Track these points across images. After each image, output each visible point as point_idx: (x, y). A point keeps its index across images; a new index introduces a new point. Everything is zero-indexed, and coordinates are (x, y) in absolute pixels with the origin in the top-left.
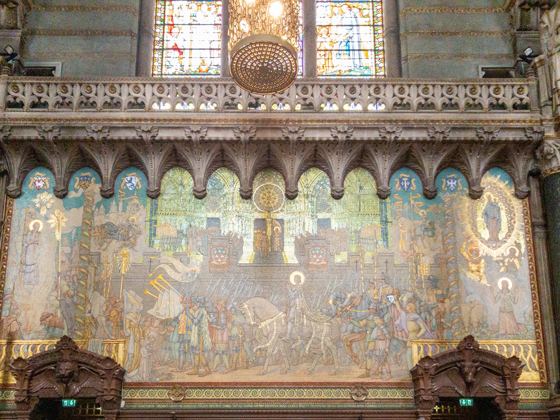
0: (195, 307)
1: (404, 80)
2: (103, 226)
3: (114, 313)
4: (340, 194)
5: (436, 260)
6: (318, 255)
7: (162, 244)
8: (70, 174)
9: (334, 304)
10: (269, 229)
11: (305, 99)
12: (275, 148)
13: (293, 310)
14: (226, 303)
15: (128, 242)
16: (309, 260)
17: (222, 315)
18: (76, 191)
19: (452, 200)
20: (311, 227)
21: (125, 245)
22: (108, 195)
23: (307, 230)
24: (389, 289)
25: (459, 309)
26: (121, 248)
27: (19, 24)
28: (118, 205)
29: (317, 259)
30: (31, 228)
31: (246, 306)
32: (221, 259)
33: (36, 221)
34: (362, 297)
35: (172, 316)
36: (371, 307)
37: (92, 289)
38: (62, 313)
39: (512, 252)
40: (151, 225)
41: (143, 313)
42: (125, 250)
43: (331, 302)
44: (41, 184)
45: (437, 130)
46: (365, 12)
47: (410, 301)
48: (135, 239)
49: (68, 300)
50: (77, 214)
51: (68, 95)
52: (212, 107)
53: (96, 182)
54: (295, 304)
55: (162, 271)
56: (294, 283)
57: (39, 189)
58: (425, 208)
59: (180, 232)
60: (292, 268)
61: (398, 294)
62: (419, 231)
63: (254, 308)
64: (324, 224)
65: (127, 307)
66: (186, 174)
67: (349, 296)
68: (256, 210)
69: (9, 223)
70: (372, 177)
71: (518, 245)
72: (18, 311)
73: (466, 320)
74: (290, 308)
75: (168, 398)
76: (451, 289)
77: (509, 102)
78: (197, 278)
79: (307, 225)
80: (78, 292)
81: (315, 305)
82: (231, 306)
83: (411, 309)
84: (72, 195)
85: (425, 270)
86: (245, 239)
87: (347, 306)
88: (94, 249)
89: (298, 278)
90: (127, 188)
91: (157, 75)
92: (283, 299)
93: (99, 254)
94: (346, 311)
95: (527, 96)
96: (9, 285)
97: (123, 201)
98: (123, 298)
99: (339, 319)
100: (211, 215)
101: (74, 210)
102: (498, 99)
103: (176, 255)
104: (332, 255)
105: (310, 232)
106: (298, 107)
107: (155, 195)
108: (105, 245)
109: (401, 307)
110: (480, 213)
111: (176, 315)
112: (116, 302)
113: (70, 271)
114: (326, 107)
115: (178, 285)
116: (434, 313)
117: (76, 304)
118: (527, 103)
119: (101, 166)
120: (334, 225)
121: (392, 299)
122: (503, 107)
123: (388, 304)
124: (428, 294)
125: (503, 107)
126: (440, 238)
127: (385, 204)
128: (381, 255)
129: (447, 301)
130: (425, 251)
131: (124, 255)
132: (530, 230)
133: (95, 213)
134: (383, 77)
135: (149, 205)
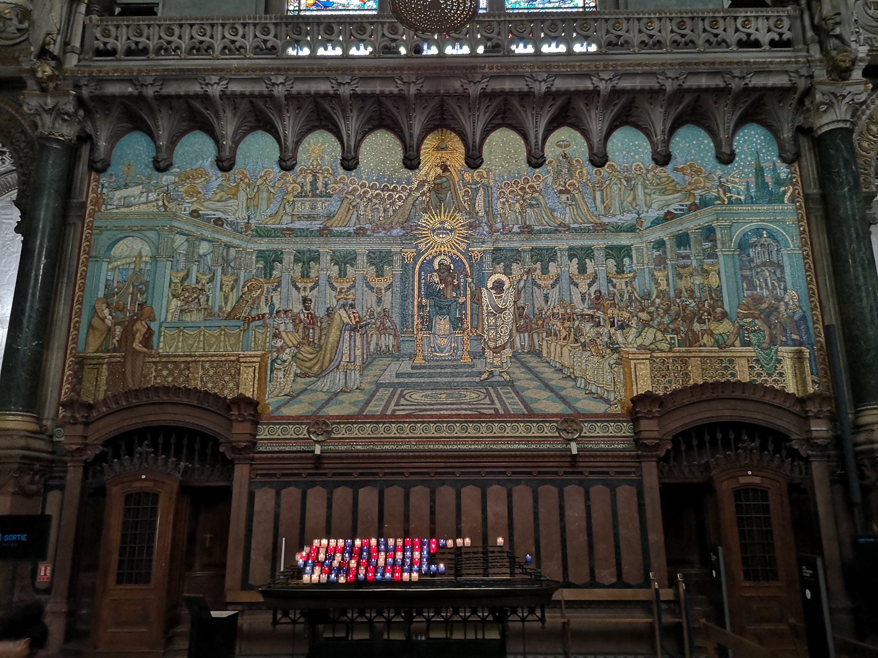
1: (620, 13)
4: (540, 161)
11: (489, 39)
12: (452, 104)
45: (669, 75)
51: (175, 38)
52: (363, 51)
75: (307, 436)
77: (765, 38)
91: (294, 11)
95: (789, 30)
102: (749, 35)
106: (481, 50)
114: (520, 49)
118: (789, 40)
122: (756, 44)
125: (756, 44)
132: (803, 204)
134: (594, 9)
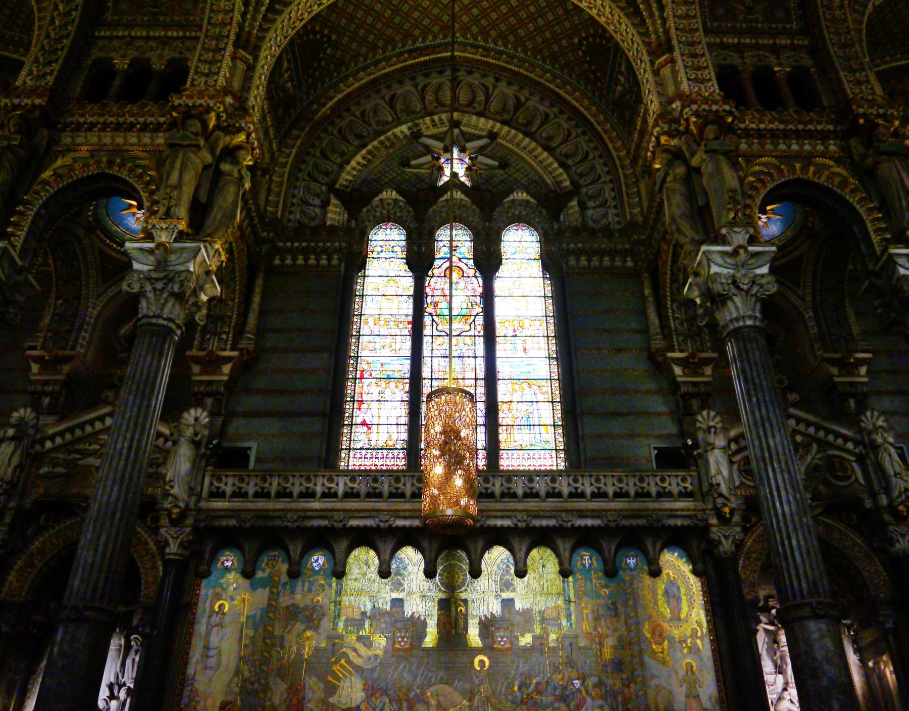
0: (377, 695)
2: (287, 608)
3: (295, 701)
5: (619, 641)
6: (502, 637)
7: (346, 626)
8: (258, 555)
9: (519, 689)
10: (453, 609)
13: (477, 697)
14: (408, 690)
15: (311, 624)
16: (494, 643)
17: (405, 704)
18: (264, 571)
19: (632, 579)
20: (495, 608)
21: (308, 628)
22: (294, 574)
23: (491, 610)
24: (574, 674)
25: (646, 694)
26: (304, 631)
27: (223, 412)
28: (303, 585)
29: (501, 640)
30: (217, 610)
31: (429, 694)
32: (405, 642)
33: (221, 602)
34: (547, 682)
35: (354, 705)
36: (557, 693)
37: (274, 675)
38: (242, 700)
39: (694, 632)
40: (335, 606)
41: (324, 701)
42: (308, 633)
43: (516, 688)
44: (229, 564)
46: (544, 389)
47: (595, 686)
48: (320, 620)
49: (249, 687)
50: (263, 595)
53: (283, 562)
54: (479, 691)
55: (345, 655)
56: (478, 669)
57: (227, 568)
58: (606, 586)
59: (364, 614)
60: (478, 651)
61: (583, 678)
62: (601, 612)
63: (437, 695)
64: (508, 604)
65: (309, 695)
66: (372, 553)
67: (534, 681)
68: (440, 590)
69: (196, 604)
70: (554, 556)
71: (700, 626)
72: (197, 698)
73: (652, 706)
74: (474, 695)
76: (636, 673)
78: (380, 663)
79: (490, 606)
80: (259, 678)
81: (500, 692)
82: (413, 693)
83: (596, 694)
84: (260, 574)
85: (608, 653)
86: (428, 621)
87: (532, 693)
88: (278, 631)
89: (482, 663)
90: (313, 568)
92: (467, 686)
93: (282, 638)
94: (532, 698)
96: (190, 671)
97: (309, 582)
98: (304, 684)
99: (524, 707)
100: (395, 595)
101: (260, 590)
103: (359, 639)
104: (517, 638)
105: (494, 612)
107: (339, 574)
108: (289, 627)
109: (587, 693)
110: (660, 592)
111: (358, 703)
112: (297, 689)
113: (253, 655)
115: (358, 670)
116: (620, 699)
117: (257, 692)
119: (291, 548)
120: (518, 605)
121: (577, 683)
123: (574, 690)
124: (613, 679)
126: (622, 617)
127: (568, 582)
128: (565, 637)
129: (632, 685)
130: (609, 632)
131: (308, 638)
133: (281, 594)
135: (334, 585)
